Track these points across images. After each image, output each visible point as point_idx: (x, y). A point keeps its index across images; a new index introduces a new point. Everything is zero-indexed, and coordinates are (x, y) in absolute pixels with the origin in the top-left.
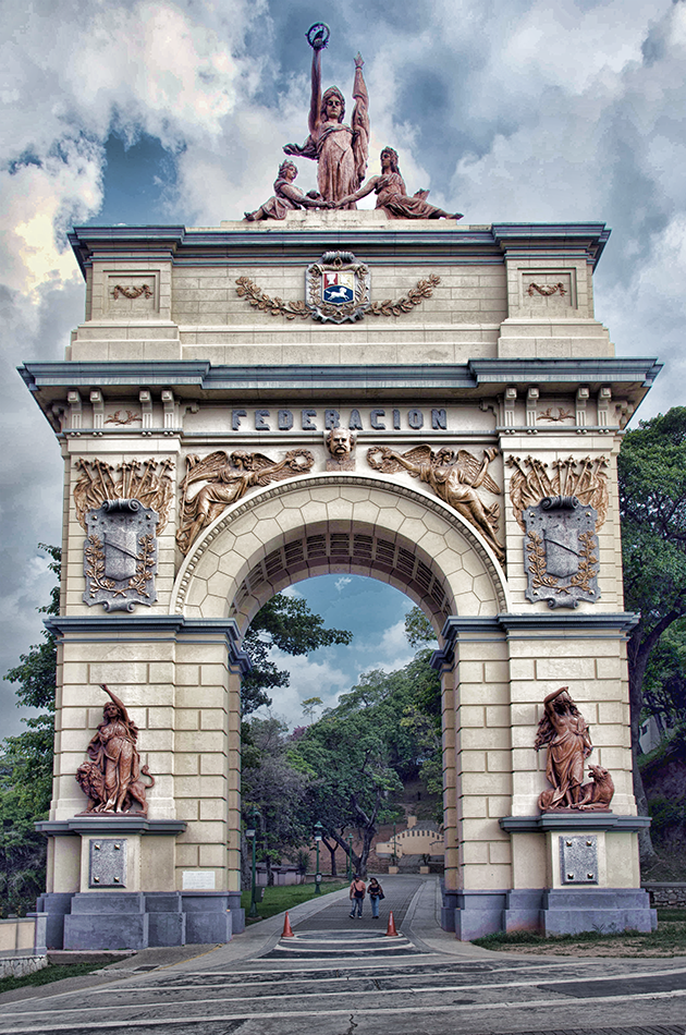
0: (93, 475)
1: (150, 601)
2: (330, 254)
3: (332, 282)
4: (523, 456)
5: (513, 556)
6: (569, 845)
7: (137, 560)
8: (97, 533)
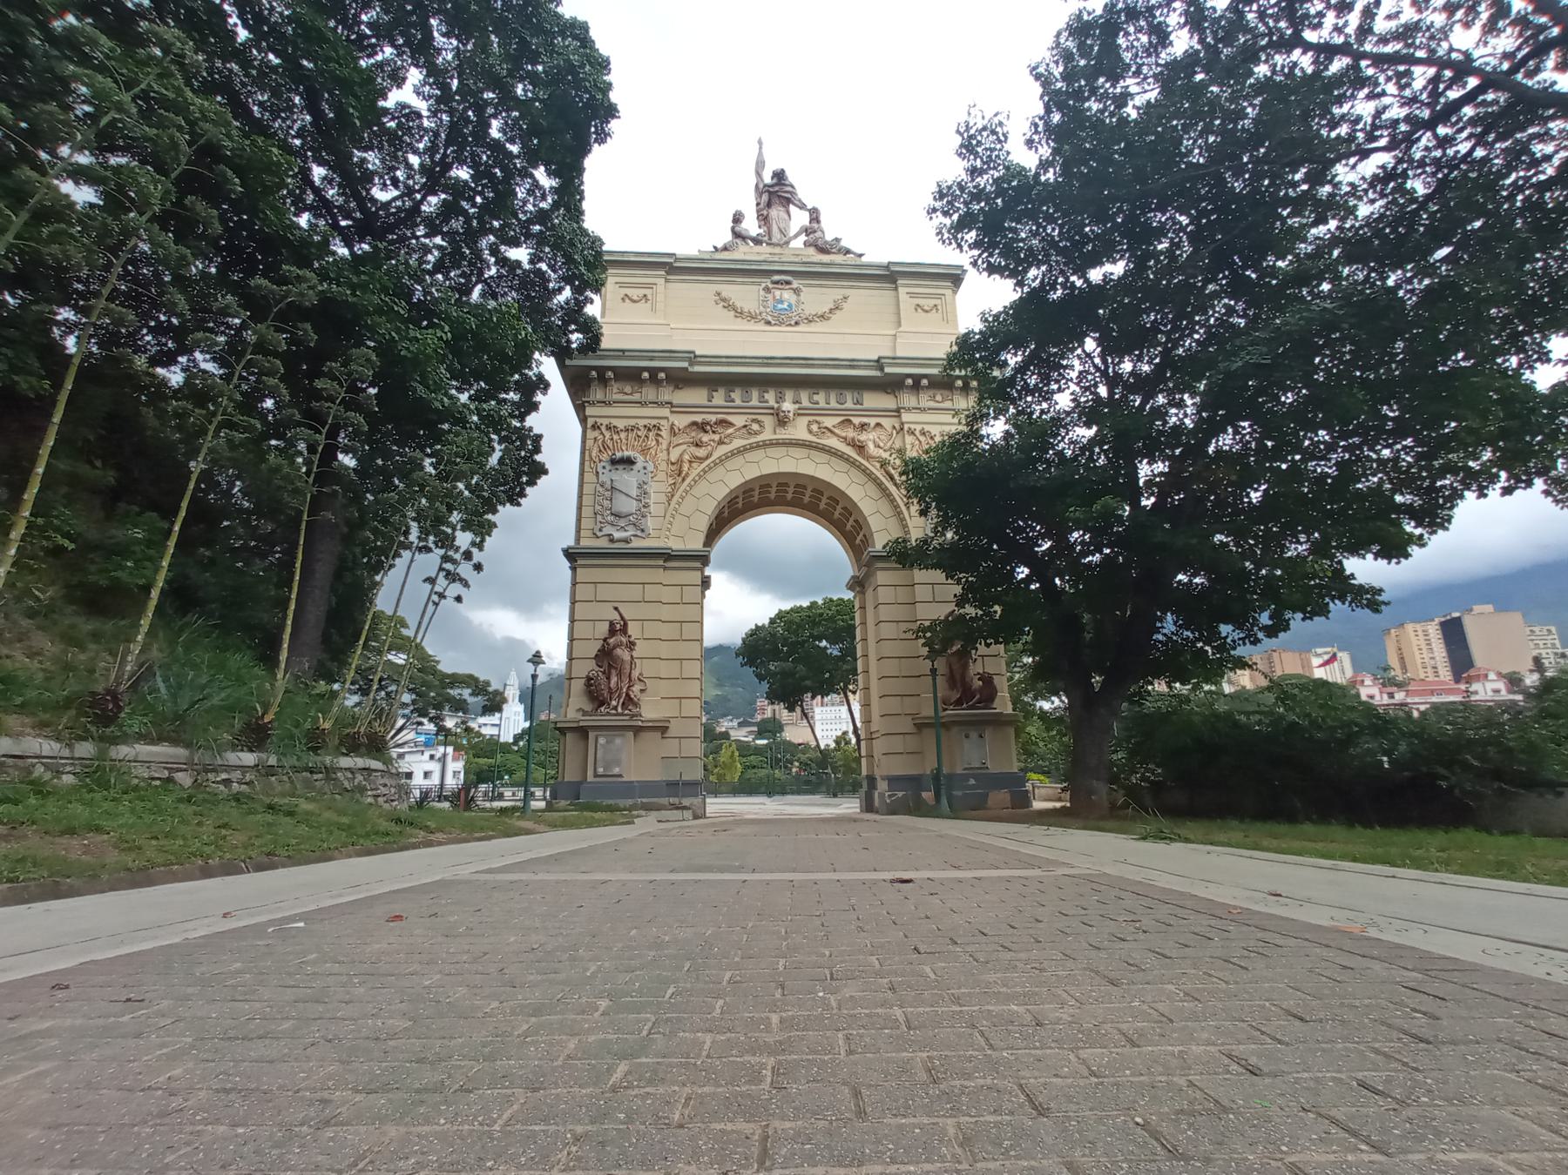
0: (608, 435)
2: (776, 278)
4: (919, 427)
8: (605, 478)
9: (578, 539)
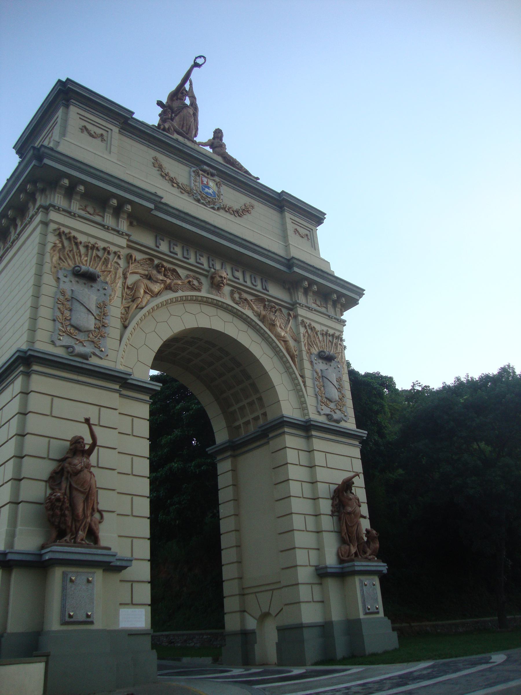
0: (66, 243)
2: (205, 167)
5: (309, 382)
6: (366, 585)
7: (95, 318)
9: (32, 342)
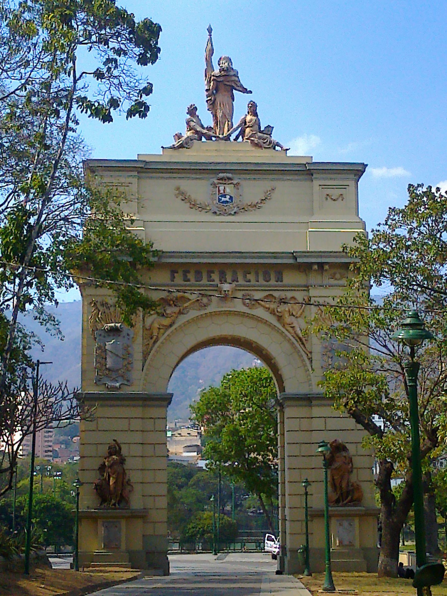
1: (129, 382)
2: (221, 175)
3: (222, 192)
